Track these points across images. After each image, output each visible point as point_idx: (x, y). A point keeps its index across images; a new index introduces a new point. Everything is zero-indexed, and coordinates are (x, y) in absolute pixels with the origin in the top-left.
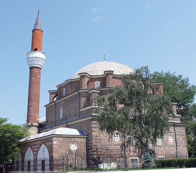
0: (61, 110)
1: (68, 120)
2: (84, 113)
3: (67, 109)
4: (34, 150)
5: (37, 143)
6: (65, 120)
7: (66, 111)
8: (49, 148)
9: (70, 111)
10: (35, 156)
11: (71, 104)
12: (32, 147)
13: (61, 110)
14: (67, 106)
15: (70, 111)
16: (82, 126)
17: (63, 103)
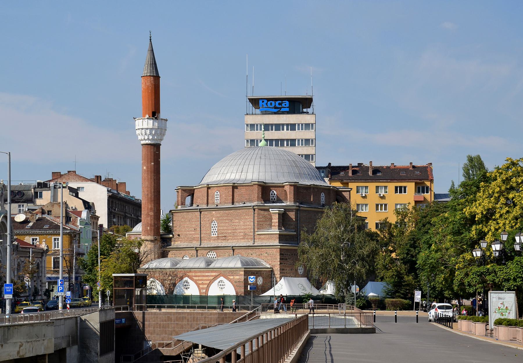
0: (215, 224)
1: (230, 241)
2: (262, 237)
3: (227, 225)
4: (200, 282)
5: (207, 274)
6: (224, 239)
7: (225, 228)
8: (236, 282)
9: (234, 230)
10: (204, 291)
11: (237, 221)
12: (195, 278)
13: (215, 224)
14: (227, 221)
15: (234, 230)
16: (261, 254)
17: (218, 215)
